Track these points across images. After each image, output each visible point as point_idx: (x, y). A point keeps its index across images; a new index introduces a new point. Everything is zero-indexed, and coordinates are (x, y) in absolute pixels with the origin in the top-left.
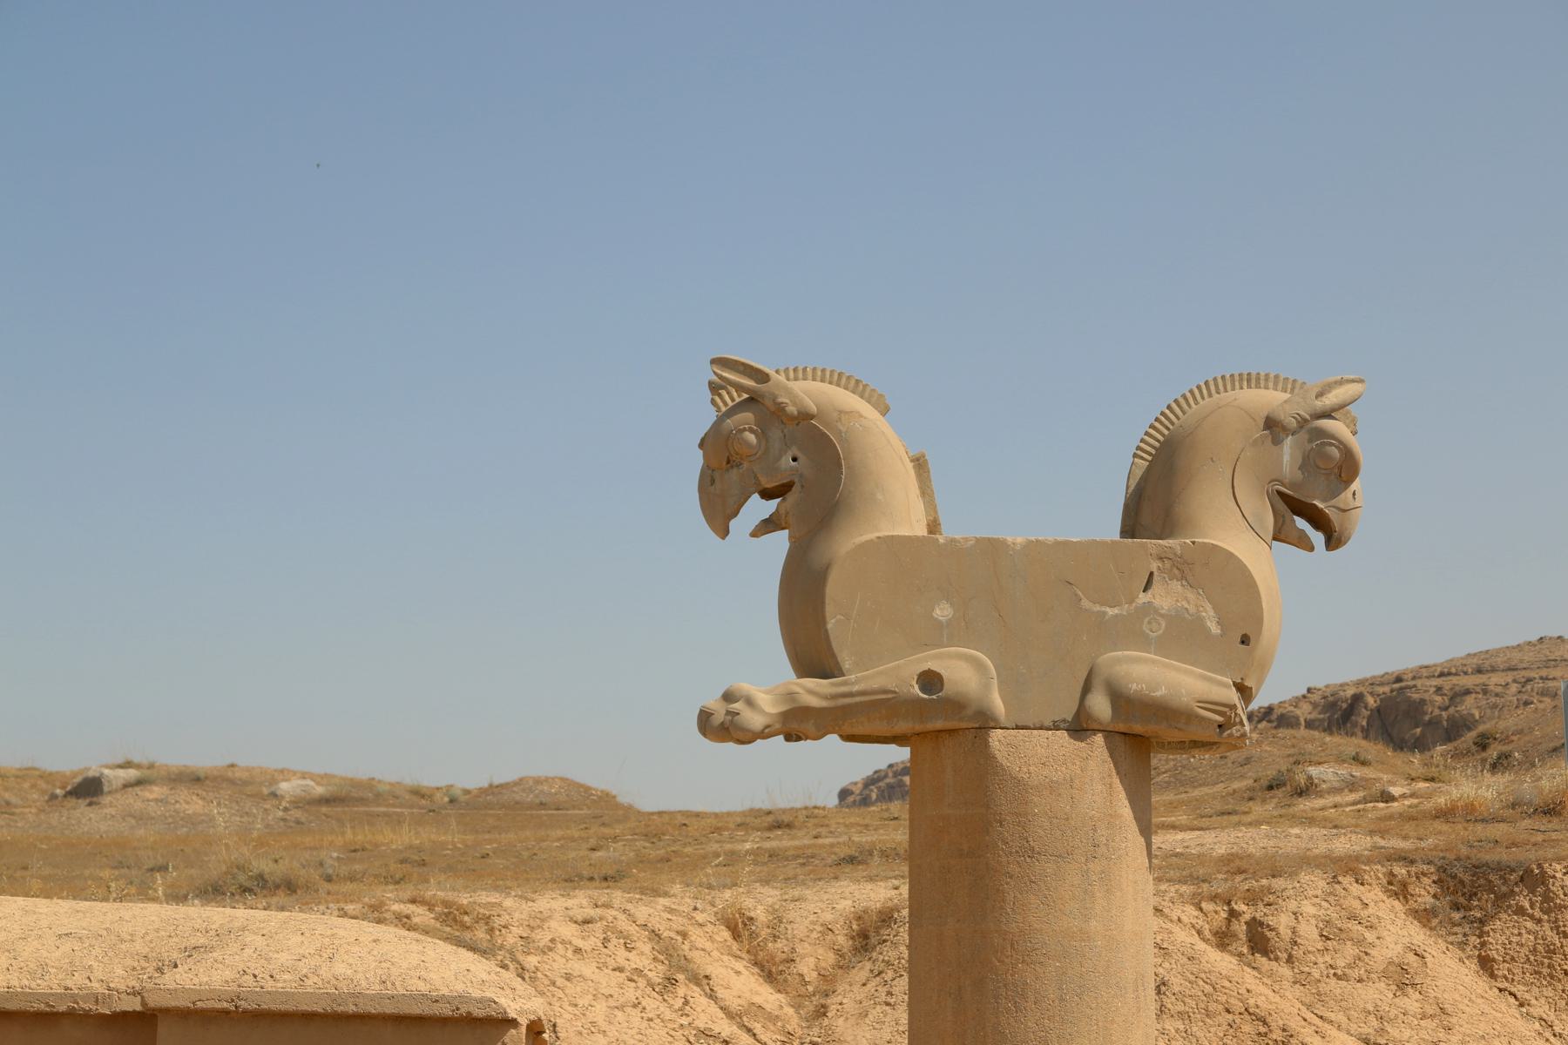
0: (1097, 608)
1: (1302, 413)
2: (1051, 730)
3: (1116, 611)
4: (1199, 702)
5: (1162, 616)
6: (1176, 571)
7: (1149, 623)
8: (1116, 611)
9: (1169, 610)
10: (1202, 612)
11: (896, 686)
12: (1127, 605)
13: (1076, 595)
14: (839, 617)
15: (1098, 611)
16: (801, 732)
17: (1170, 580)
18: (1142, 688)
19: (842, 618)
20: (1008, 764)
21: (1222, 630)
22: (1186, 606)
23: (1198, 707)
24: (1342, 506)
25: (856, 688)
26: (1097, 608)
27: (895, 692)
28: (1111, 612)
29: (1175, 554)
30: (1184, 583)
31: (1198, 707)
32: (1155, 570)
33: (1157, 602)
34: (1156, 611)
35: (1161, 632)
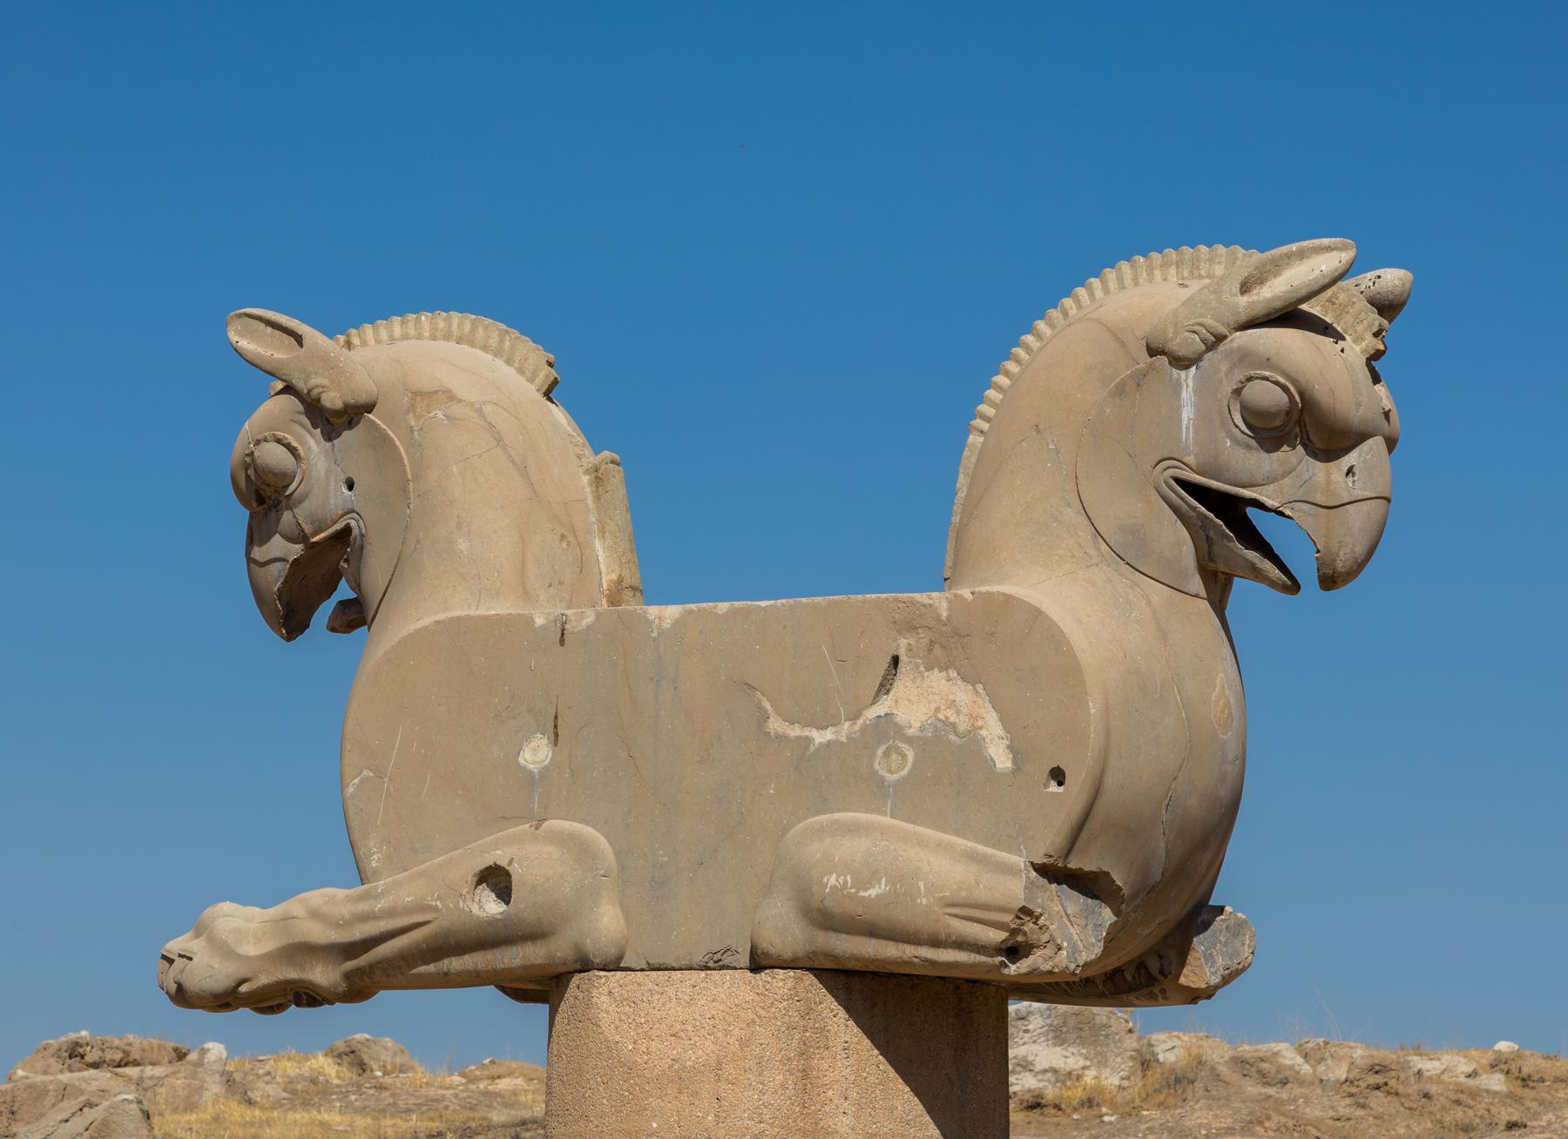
0: (795, 731)
1: (1209, 321)
2: (709, 969)
3: (828, 735)
4: (953, 905)
5: (910, 740)
6: (938, 651)
7: (886, 754)
8: (828, 735)
9: (922, 729)
10: (980, 728)
11: (439, 898)
12: (847, 724)
13: (760, 708)
14: (366, 773)
15: (798, 738)
16: (312, 990)
17: (927, 670)
18: (845, 882)
19: (371, 774)
20: (617, 1038)
21: (1014, 761)
22: (953, 719)
23: (955, 916)
24: (1320, 499)
25: (380, 905)
26: (795, 731)
27: (436, 909)
28: (820, 737)
29: (938, 617)
30: (953, 673)
31: (955, 916)
32: (902, 653)
33: (902, 717)
34: (899, 731)
35: (905, 772)
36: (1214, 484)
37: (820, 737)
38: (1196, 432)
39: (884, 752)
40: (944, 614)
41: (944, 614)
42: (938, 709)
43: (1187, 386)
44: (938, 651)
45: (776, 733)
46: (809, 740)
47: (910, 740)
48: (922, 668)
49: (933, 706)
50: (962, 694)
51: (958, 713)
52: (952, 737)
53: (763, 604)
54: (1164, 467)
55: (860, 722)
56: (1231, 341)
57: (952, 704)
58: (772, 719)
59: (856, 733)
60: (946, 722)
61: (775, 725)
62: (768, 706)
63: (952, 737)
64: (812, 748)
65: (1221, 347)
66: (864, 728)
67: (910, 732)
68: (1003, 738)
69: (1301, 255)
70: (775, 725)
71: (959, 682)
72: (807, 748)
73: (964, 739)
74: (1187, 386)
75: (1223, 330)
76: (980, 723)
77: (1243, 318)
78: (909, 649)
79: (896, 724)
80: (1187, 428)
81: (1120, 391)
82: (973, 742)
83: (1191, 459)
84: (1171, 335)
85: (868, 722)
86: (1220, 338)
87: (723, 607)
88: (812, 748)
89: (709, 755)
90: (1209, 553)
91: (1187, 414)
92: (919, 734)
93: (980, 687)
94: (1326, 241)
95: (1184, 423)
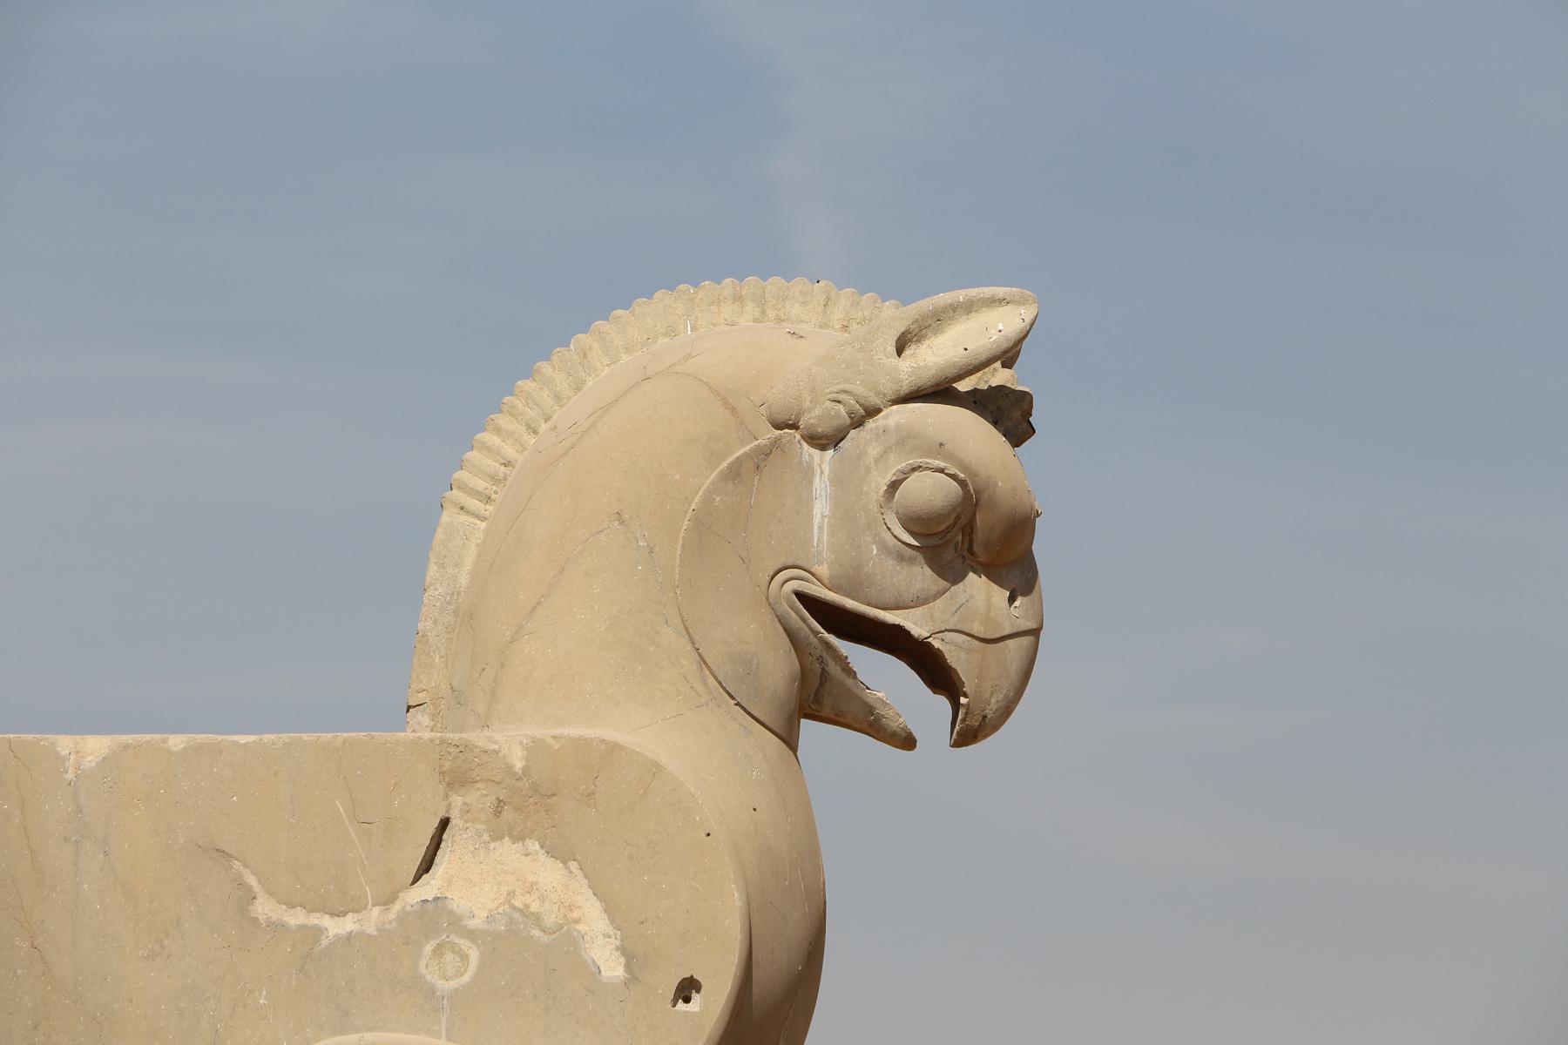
0: (297, 918)
3: (348, 924)
5: (472, 935)
8: (348, 924)
9: (490, 919)
26: (297, 918)
28: (336, 927)
29: (509, 769)
33: (459, 902)
34: (456, 922)
36: (850, 603)
37: (336, 927)
38: (832, 534)
39: (434, 951)
40: (519, 765)
41: (519, 765)
42: (512, 894)
43: (822, 472)
44: (508, 815)
45: (268, 919)
46: (319, 931)
47: (472, 935)
48: (486, 837)
49: (505, 889)
50: (548, 873)
51: (542, 899)
52: (536, 933)
53: (242, 739)
54: (786, 577)
55: (396, 908)
56: (886, 417)
57: (531, 888)
58: (259, 900)
59: (390, 923)
60: (524, 912)
61: (264, 908)
62: (253, 881)
63: (536, 933)
64: (324, 942)
65: (871, 424)
66: (403, 918)
67: (474, 923)
68: (609, 937)
69: (969, 307)
70: (264, 908)
71: (542, 856)
72: (317, 941)
73: (554, 936)
74: (822, 472)
75: (875, 401)
76: (576, 914)
77: (905, 388)
78: (466, 810)
79: (451, 913)
80: (820, 528)
81: (735, 473)
82: (567, 940)
83: (823, 570)
84: (808, 403)
85: (408, 908)
86: (873, 412)
87: (177, 742)
88: (324, 942)
89: (163, 948)
90: (817, 691)
91: (821, 509)
92: (485, 926)
93: (574, 866)
94: (1000, 291)
95: (817, 521)
